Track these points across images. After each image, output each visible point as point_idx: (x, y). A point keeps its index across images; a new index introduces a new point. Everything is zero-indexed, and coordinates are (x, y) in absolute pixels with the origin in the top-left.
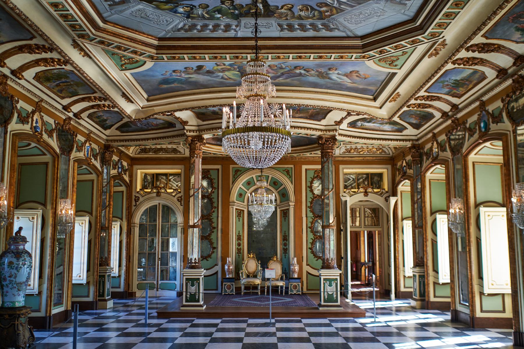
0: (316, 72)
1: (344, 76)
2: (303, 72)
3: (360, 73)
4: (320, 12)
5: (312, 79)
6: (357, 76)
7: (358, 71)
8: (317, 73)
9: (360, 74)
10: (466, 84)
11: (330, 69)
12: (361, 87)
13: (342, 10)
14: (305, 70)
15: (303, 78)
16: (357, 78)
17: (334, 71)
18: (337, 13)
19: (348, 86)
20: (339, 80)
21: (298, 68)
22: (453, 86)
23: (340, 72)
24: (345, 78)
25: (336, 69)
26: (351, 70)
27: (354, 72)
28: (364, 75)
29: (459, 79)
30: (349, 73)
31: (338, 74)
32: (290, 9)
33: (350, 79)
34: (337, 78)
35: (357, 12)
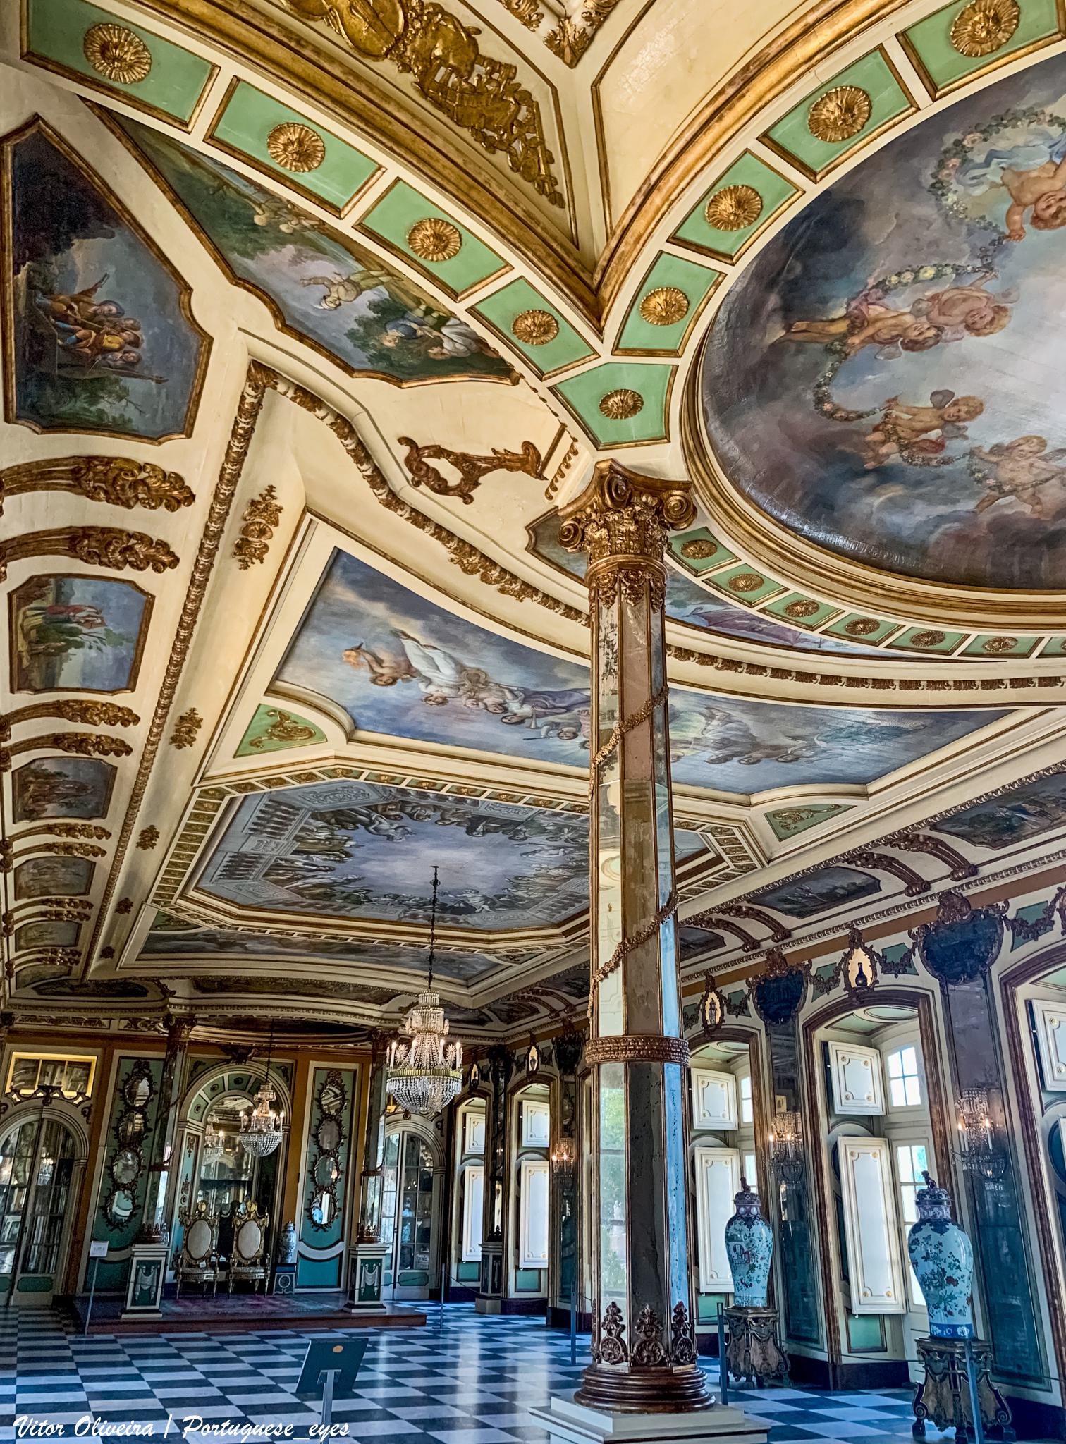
0: (482, 700)
1: (417, 671)
2: (514, 707)
3: (369, 675)
4: (402, 810)
5: (511, 677)
6: (380, 662)
7: (374, 681)
8: (482, 695)
9: (371, 668)
10: (38, 642)
11: (444, 701)
12: (379, 610)
13: (369, 808)
14: (506, 710)
15: (532, 684)
16: (382, 655)
17: (436, 694)
18: (376, 806)
19: (419, 624)
20: (438, 657)
21: (515, 720)
22: (68, 620)
23: (422, 686)
24: (417, 663)
25: (426, 699)
26: (390, 688)
27: (384, 679)
28: (357, 665)
29: (72, 651)
30: (399, 681)
31: (429, 681)
32: (443, 819)
33: (404, 654)
34: (437, 668)
35: (346, 802)
